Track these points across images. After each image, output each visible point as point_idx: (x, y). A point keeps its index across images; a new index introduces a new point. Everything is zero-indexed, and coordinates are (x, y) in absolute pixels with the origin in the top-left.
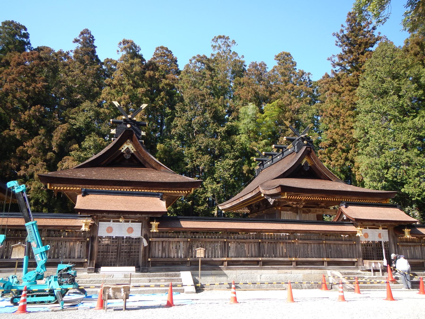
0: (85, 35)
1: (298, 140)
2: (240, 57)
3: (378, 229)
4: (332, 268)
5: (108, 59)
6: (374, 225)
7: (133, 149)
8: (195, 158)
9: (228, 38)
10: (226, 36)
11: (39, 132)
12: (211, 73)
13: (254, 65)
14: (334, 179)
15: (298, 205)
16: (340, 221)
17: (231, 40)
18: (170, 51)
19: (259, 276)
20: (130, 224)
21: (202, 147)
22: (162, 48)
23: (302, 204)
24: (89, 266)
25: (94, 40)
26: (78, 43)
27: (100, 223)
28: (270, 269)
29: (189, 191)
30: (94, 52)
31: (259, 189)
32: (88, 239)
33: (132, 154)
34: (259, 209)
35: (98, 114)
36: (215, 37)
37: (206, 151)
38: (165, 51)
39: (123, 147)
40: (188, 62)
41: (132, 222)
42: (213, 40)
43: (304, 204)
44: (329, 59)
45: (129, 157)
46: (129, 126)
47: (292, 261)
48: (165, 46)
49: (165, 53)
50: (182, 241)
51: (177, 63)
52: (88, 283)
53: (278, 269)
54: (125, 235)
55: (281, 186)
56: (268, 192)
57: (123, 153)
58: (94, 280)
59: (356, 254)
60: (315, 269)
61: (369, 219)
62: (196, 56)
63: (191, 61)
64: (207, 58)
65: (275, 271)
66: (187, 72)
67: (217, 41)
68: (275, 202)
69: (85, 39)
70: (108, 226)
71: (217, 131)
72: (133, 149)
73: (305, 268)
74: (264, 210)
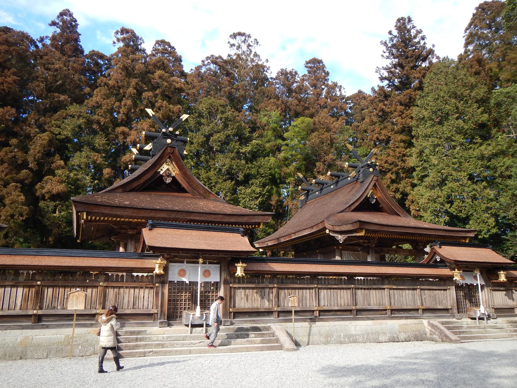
0: (65, 17)
4: (427, 316)
6: (467, 267)
9: (249, 36)
10: (247, 33)
11: (10, 142)
13: (284, 73)
14: (402, 215)
15: (370, 244)
16: (431, 263)
17: (252, 39)
18: (173, 48)
19: (353, 327)
22: (163, 42)
24: (160, 319)
25: (77, 25)
26: (55, 27)
27: (171, 264)
28: (365, 320)
29: (257, 226)
30: (77, 40)
33: (174, 178)
35: (89, 122)
36: (234, 33)
38: (166, 46)
39: (161, 168)
40: (200, 63)
41: (210, 263)
42: (231, 36)
45: (170, 181)
46: (169, 141)
47: (386, 310)
48: (167, 40)
49: (166, 49)
51: (182, 63)
53: (373, 320)
55: (360, 222)
56: (337, 229)
57: (162, 176)
58: (173, 337)
59: (450, 300)
60: (410, 318)
61: (477, 261)
63: (203, 61)
65: (370, 322)
69: (64, 22)
70: (180, 268)
71: (241, 151)
74: (317, 249)
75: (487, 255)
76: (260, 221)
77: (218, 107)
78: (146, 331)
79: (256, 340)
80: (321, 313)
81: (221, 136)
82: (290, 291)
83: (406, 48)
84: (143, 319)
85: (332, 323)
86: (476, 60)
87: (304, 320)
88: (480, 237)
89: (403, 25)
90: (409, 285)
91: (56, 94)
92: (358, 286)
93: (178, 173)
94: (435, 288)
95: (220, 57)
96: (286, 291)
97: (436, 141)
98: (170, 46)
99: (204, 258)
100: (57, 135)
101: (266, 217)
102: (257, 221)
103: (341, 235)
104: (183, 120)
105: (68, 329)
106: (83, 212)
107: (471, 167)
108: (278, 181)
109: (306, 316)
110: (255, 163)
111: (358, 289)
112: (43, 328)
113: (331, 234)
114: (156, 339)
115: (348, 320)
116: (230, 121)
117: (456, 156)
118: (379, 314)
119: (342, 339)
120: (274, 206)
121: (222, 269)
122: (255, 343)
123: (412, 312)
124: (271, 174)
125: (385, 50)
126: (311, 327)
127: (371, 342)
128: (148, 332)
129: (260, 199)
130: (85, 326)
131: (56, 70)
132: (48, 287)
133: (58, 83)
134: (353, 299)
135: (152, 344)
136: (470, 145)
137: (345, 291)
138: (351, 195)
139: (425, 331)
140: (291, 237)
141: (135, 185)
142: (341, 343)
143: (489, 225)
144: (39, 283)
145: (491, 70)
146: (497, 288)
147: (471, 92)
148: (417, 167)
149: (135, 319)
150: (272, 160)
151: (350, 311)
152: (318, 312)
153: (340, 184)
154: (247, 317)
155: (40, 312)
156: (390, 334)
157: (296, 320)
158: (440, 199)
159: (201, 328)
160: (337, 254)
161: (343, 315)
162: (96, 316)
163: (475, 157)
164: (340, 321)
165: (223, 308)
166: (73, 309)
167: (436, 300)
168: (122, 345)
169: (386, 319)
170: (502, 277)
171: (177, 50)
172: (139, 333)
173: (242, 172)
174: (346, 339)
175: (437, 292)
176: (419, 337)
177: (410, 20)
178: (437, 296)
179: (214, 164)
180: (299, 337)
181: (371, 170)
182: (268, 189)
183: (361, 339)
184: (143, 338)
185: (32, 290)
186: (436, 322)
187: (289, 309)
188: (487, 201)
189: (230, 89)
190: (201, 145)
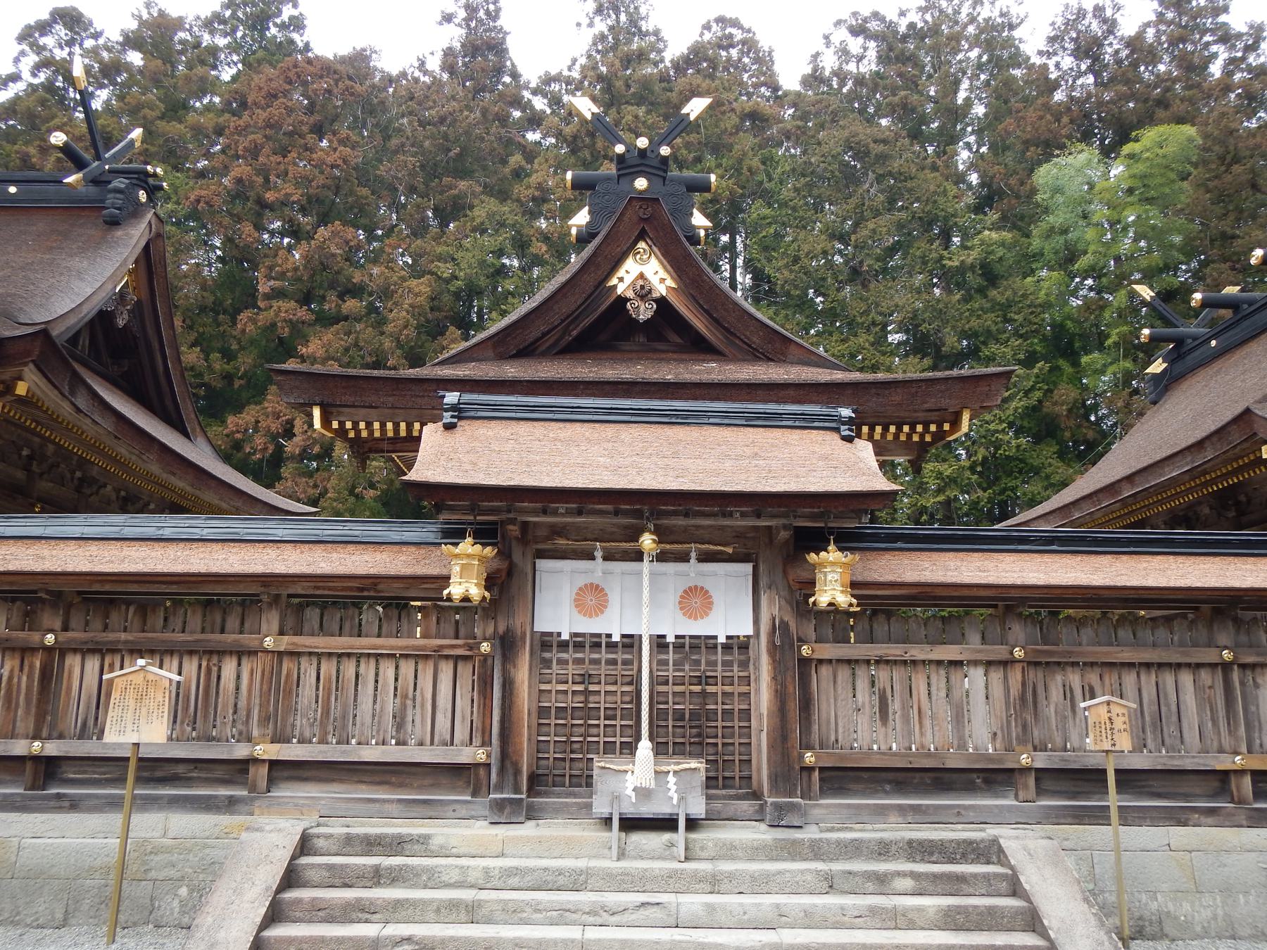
5: (547, 73)
7: (662, 281)
18: (749, 31)
20: (694, 571)
22: (721, 20)
24: (500, 788)
27: (543, 565)
29: (946, 427)
32: (485, 647)
33: (662, 302)
39: (621, 273)
41: (705, 558)
45: (649, 314)
46: (641, 183)
50: (975, 663)
52: (496, 883)
54: (674, 626)
57: (622, 300)
70: (581, 581)
72: (662, 281)
78: (424, 840)
79: (920, 909)
82: (1093, 677)
84: (435, 786)
91: (447, 180)
93: (673, 285)
96: (1075, 679)
98: (741, 27)
99: (662, 535)
100: (448, 281)
104: (692, 118)
105: (146, 815)
106: (311, 405)
109: (1186, 797)
112: (59, 809)
114: (454, 876)
121: (763, 582)
122: (912, 926)
128: (436, 842)
130: (208, 805)
131: (442, 120)
132: (86, 651)
133: (451, 154)
135: (424, 903)
140: (1119, 493)
141: (534, 334)
144: (50, 639)
149: (401, 786)
152: (1247, 781)
154: (887, 794)
155: (52, 748)
157: (1129, 817)
159: (667, 836)
162: (252, 770)
165: (771, 747)
166: (122, 739)
168: (299, 901)
171: (757, 37)
172: (396, 845)
180: (1153, 895)
182: (1041, 369)
184: (401, 868)
185: (32, 667)
187: (1092, 762)
189: (906, 97)
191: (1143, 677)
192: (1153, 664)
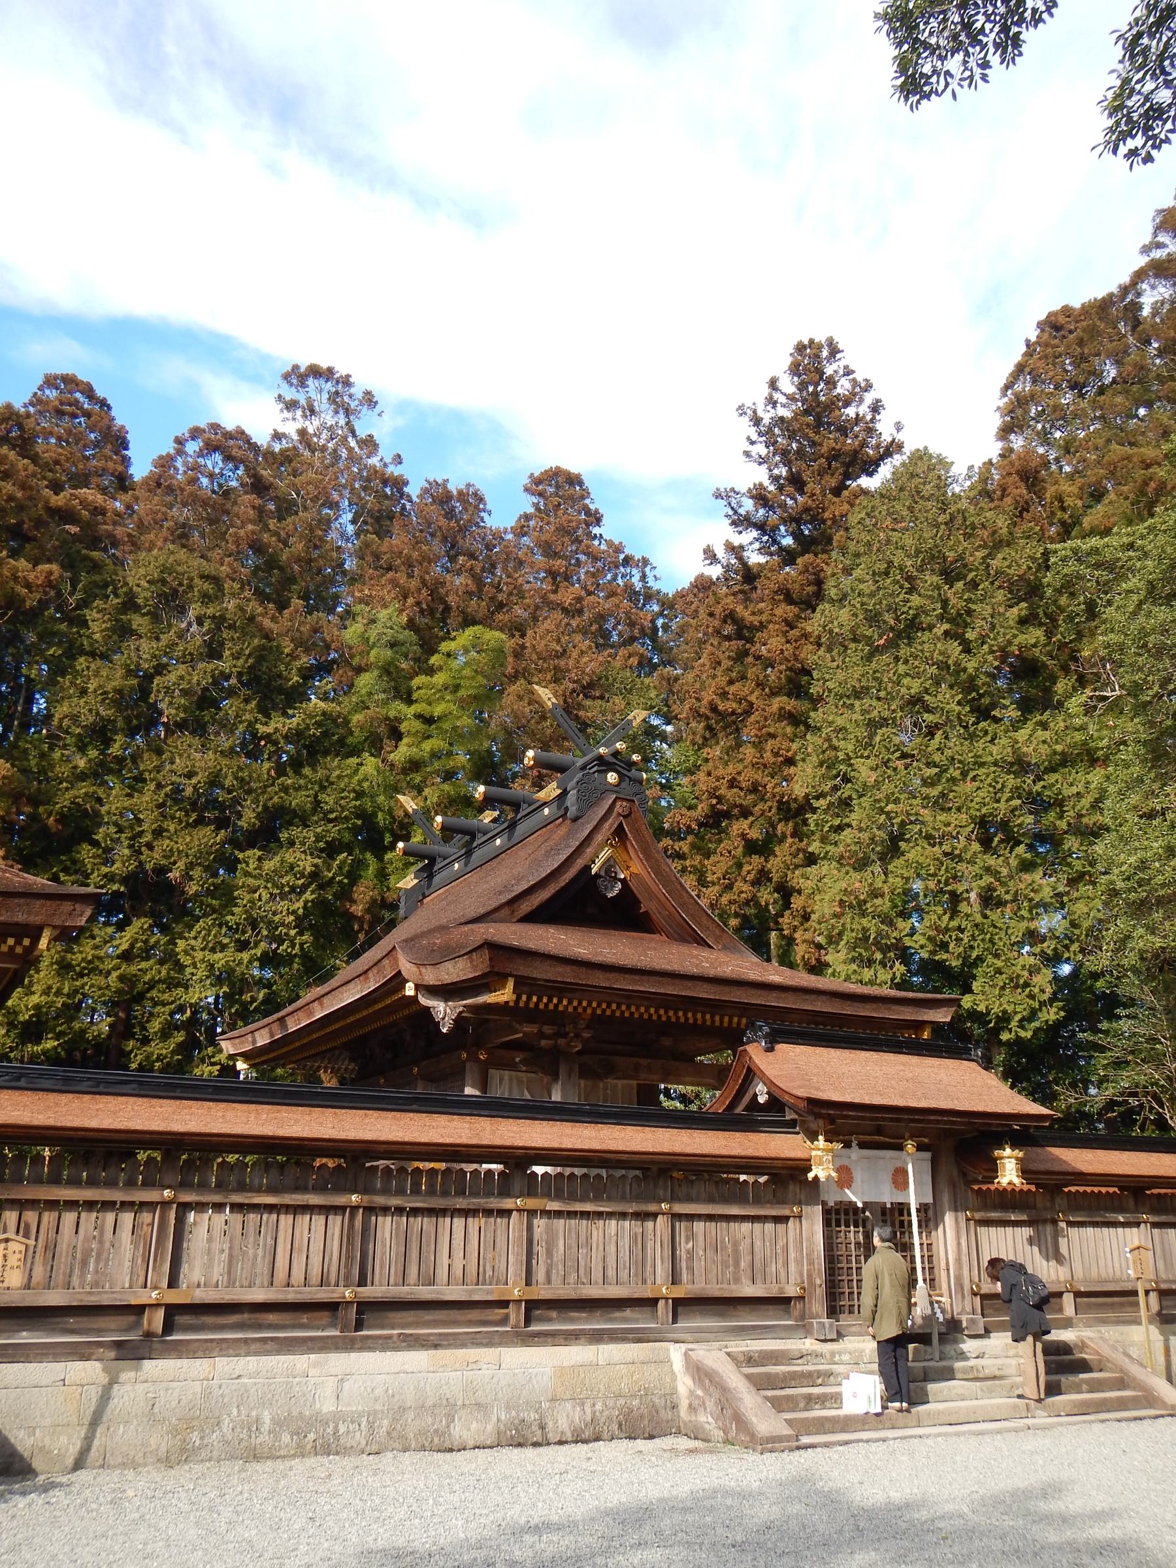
1: (583, 768)
2: (388, 460)
3: (900, 1148)
6: (879, 1131)
8: (147, 837)
10: (341, 370)
12: (258, 502)
13: (440, 496)
14: (718, 939)
15: (561, 1042)
19: (331, 1383)
21: (189, 791)
23: (577, 1036)
28: (396, 1349)
29: (26, 942)
31: (396, 960)
34: (387, 1052)
37: (207, 808)
40: (169, 448)
42: (286, 377)
43: (586, 1035)
44: (718, 495)
47: (504, 1304)
53: (436, 1346)
55: (491, 946)
56: (431, 977)
59: (799, 1262)
62: (203, 425)
63: (179, 442)
64: (248, 440)
65: (417, 1359)
66: (159, 482)
67: (303, 384)
68: (459, 1021)
71: (262, 729)
73: (571, 1337)
75: (969, 1087)
76: (36, 919)
77: (191, 579)
80: (181, 1319)
81: (200, 675)
82: (31, 1216)
83: (820, 437)
85: (225, 1365)
86: (1018, 473)
87: (81, 1353)
88: (1005, 1036)
89: (811, 361)
90: (623, 1198)
92: (380, 1200)
94: (734, 1210)
95: (240, 434)
97: (878, 710)
101: (67, 906)
102: (20, 918)
103: (446, 1001)
107: (976, 794)
108: (388, 838)
109: (99, 1332)
110: (307, 771)
111: (385, 1210)
113: (424, 1001)
115: (311, 1350)
116: (230, 627)
117: (937, 757)
118: (471, 1323)
119: (264, 1438)
120: (361, 920)
123: (628, 1313)
124: (360, 813)
125: (754, 437)
126: (113, 1381)
127: (405, 1450)
129: (308, 896)
134: (350, 1258)
136: (983, 724)
137: (319, 1220)
138: (527, 864)
139: (674, 1391)
140: (311, 1014)
142: (255, 1455)
143: (1031, 996)
145: (1061, 501)
146: (994, 1215)
147: (991, 556)
148: (817, 798)
150: (370, 764)
151: (332, 1307)
152: (161, 1313)
153: (521, 829)
156: (508, 1408)
158: (878, 901)
160: (468, 1079)
161: (293, 1327)
163: (995, 764)
164: (268, 1353)
167: (737, 1264)
169: (500, 1344)
170: (1009, 1171)
173: (256, 801)
174: (286, 1438)
175: (746, 1227)
176: (643, 1423)
177: (834, 351)
178: (744, 1247)
179: (158, 769)
181: (612, 777)
182: (343, 862)
183: (359, 1438)
186: (722, 1355)
188: (1030, 911)
189: (253, 532)
190: (112, 700)
191: (83, 1215)
192: (96, 1202)
